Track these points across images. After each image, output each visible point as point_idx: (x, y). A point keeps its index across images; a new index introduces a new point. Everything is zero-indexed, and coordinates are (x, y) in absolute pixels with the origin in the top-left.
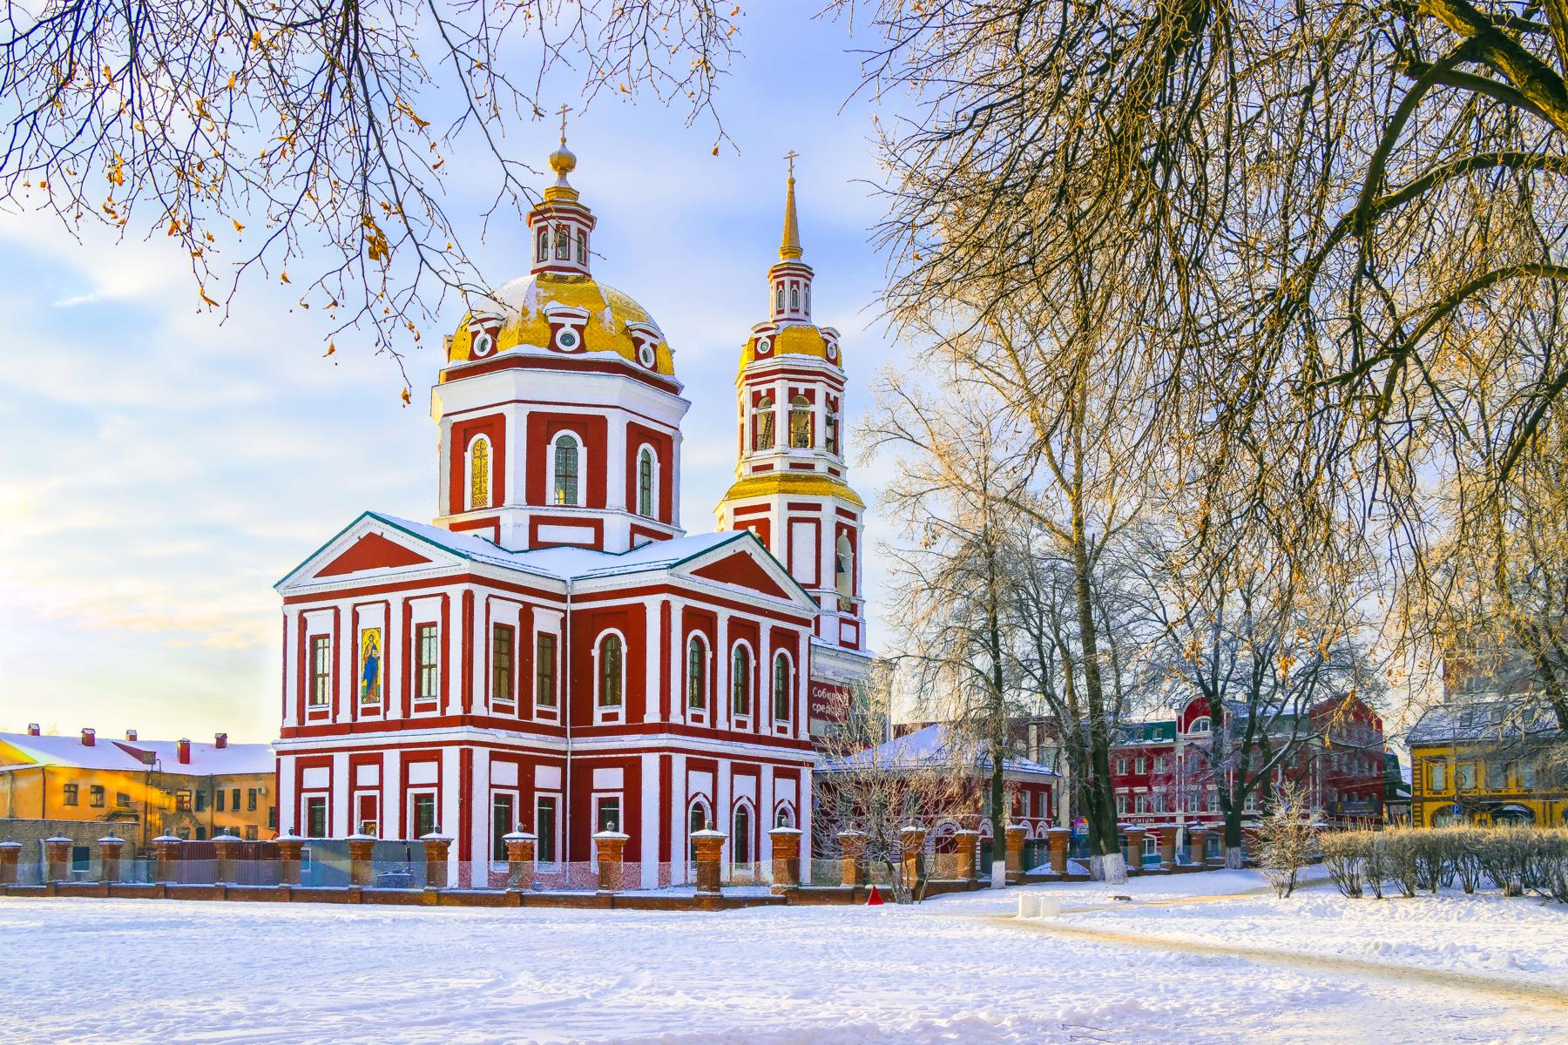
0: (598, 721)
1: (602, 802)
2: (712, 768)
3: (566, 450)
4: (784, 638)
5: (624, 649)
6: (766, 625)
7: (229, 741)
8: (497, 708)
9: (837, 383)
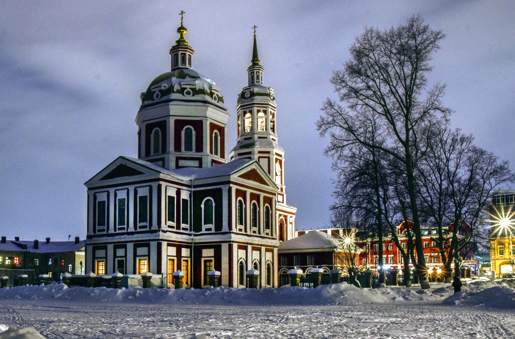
0: (204, 231)
1: (205, 261)
2: (246, 248)
4: (268, 200)
5: (214, 205)
6: (262, 195)
7: (51, 241)
8: (169, 227)
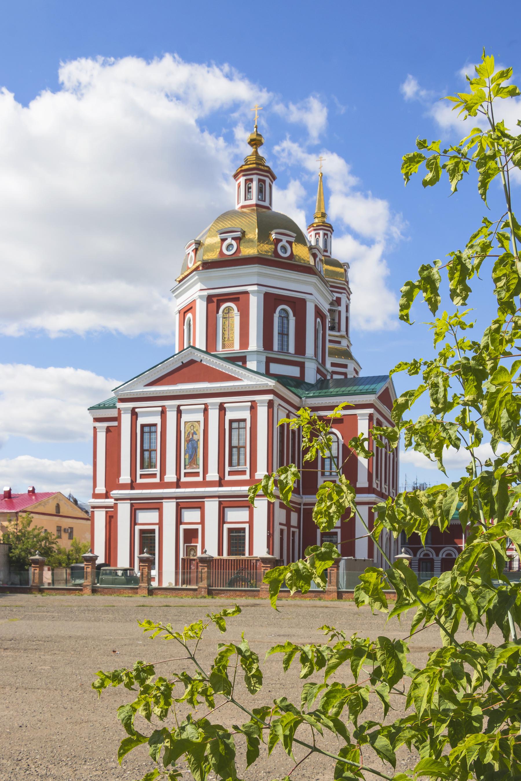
3: (284, 317)
9: (349, 293)
